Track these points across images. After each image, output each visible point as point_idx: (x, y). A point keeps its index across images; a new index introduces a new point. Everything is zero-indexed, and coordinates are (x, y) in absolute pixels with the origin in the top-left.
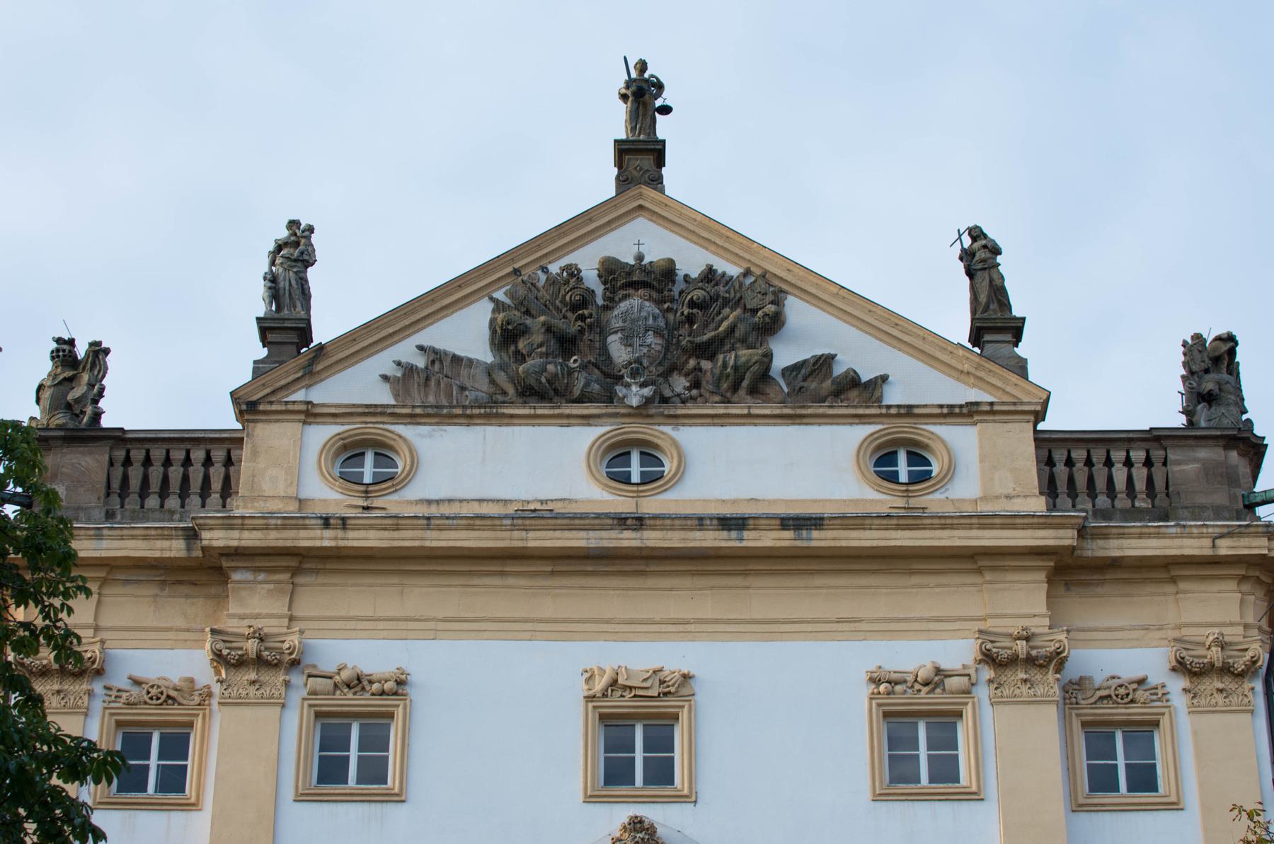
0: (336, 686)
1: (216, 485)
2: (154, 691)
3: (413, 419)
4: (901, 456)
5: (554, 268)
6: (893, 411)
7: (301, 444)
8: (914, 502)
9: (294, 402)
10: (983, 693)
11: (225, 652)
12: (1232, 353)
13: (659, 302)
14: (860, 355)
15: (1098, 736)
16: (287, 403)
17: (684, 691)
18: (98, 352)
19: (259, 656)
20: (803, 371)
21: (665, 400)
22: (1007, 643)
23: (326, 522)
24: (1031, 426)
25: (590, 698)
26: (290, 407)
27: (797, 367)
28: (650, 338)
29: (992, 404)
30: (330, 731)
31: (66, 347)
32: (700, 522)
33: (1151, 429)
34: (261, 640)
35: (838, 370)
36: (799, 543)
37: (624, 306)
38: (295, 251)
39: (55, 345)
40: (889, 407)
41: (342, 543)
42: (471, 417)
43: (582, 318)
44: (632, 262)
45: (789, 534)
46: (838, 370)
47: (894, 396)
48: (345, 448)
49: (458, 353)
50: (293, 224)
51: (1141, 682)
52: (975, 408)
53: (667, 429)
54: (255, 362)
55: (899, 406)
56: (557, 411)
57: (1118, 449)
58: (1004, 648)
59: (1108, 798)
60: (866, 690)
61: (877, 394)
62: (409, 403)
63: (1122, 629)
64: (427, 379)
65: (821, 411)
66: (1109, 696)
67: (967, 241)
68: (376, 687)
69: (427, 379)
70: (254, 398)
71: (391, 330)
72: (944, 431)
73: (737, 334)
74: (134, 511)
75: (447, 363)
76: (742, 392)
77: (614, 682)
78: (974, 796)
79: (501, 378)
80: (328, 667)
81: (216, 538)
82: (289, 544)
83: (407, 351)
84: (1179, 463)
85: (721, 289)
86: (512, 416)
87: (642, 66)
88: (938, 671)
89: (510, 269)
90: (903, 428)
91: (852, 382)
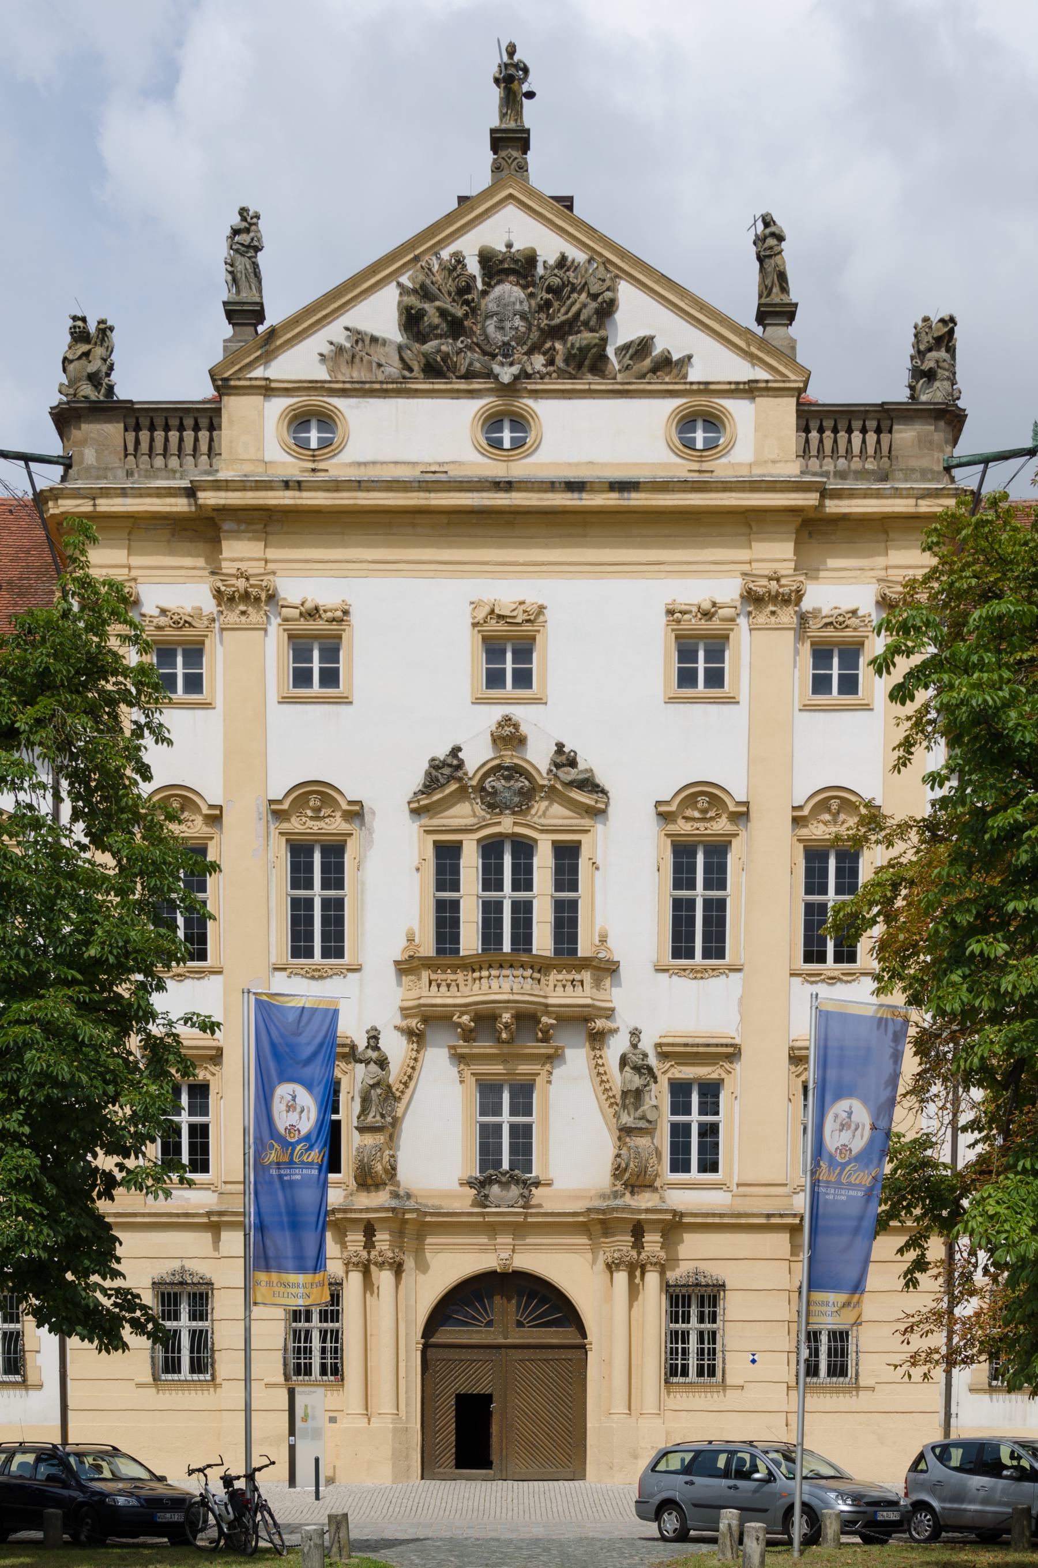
0: (301, 614)
1: (204, 447)
2: (176, 617)
3: (344, 393)
4: (701, 421)
5: (445, 254)
6: (695, 387)
7: (261, 414)
8: (705, 466)
9: (256, 379)
10: (743, 621)
11: (223, 589)
12: (951, 332)
13: (524, 287)
14: (674, 335)
15: (821, 655)
16: (251, 379)
17: (541, 618)
18: (105, 330)
19: (246, 592)
20: (631, 351)
21: (528, 376)
22: (764, 582)
23: (287, 485)
24: (794, 400)
25: (475, 625)
26: (254, 383)
27: (626, 347)
28: (518, 322)
29: (767, 381)
30: (300, 647)
31: (80, 323)
32: (551, 486)
33: (883, 404)
34: (247, 579)
35: (657, 350)
36: (622, 502)
37: (498, 290)
38: (245, 239)
39: (71, 323)
40: (692, 383)
41: (299, 502)
42: (386, 391)
43: (467, 303)
44: (504, 249)
45: (615, 495)
46: (657, 350)
47: (695, 374)
48: (295, 417)
49: (376, 334)
50: (243, 212)
51: (854, 612)
52: (754, 385)
53: (530, 402)
54: (225, 341)
55: (699, 383)
56: (449, 386)
57: (857, 419)
58: (761, 586)
59: (822, 699)
60: (663, 619)
61: (684, 371)
62: (340, 378)
63: (845, 569)
64: (353, 356)
65: (641, 387)
66: (831, 623)
67: (760, 226)
68: (329, 614)
69: (353, 356)
70: (226, 375)
71: (324, 313)
72: (730, 405)
73: (582, 318)
74: (146, 470)
75: (367, 340)
76: (585, 369)
77: (492, 612)
78: (732, 701)
79: (408, 354)
80: (294, 599)
81: (208, 498)
82: (261, 502)
83: (335, 332)
84: (901, 432)
85: (571, 274)
86: (417, 390)
87: (512, 50)
88: (714, 604)
89: (411, 256)
90: (701, 402)
91: (665, 363)
